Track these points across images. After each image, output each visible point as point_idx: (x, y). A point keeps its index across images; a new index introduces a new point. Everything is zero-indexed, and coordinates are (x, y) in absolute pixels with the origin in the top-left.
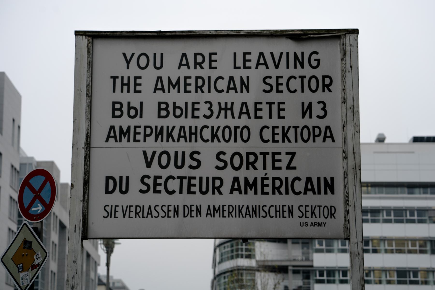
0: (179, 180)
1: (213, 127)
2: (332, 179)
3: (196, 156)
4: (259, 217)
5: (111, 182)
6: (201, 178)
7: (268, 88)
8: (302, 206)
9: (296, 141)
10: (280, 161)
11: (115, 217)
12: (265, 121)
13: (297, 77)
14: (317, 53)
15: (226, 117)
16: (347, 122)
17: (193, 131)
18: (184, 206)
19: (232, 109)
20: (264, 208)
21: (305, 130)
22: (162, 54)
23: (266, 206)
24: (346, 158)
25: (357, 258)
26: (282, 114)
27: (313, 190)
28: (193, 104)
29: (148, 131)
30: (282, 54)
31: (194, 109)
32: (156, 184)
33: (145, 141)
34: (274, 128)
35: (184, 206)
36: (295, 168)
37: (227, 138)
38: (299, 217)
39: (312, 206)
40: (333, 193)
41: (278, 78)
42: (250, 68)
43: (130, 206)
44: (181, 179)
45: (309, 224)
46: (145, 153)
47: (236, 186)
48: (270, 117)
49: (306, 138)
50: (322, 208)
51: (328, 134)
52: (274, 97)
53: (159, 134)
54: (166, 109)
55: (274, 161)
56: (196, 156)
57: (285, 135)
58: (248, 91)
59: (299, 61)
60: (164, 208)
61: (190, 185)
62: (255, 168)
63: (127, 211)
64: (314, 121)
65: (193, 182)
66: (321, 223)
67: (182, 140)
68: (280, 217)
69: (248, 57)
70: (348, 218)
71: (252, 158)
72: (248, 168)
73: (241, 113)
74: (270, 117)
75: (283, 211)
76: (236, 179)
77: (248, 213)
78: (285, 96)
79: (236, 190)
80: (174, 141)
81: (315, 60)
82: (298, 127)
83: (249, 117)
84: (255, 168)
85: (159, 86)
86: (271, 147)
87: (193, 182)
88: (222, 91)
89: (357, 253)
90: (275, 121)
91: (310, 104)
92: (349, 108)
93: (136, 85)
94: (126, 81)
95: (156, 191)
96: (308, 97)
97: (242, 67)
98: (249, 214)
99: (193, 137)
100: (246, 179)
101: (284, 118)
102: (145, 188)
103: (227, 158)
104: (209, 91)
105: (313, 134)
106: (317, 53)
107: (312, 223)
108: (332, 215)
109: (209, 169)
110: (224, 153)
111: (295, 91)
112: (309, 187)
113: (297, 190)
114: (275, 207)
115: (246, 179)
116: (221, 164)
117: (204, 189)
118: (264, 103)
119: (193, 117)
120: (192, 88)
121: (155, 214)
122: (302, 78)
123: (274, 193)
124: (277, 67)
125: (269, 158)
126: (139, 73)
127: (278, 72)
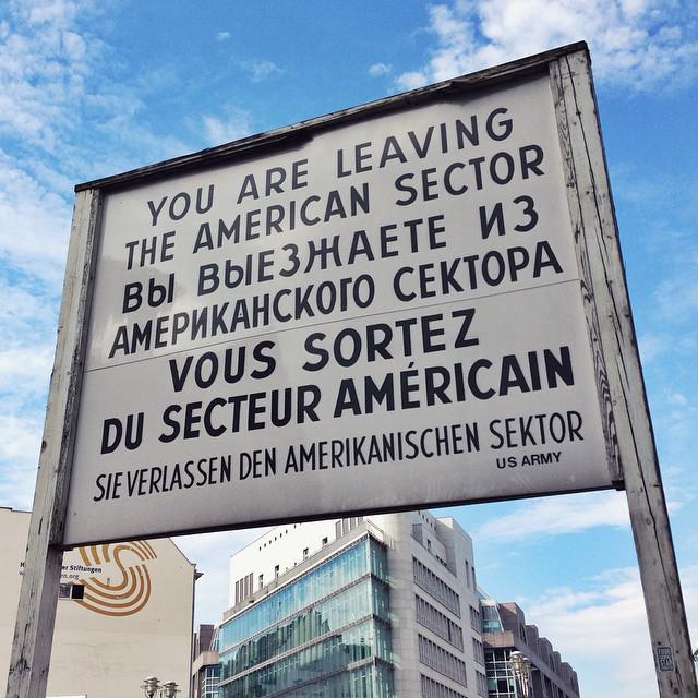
0: (233, 404)
1: (298, 291)
2: (565, 351)
3: (265, 352)
4: (401, 458)
5: (113, 429)
6: (275, 394)
7: (407, 196)
8: (499, 421)
9: (474, 286)
10: (441, 332)
11: (115, 497)
12: (406, 258)
13: (466, 163)
14: (503, 111)
15: (324, 266)
16: (582, 223)
17: (261, 305)
18: (242, 455)
19: (335, 250)
20: (411, 437)
21: (493, 262)
22: (212, 188)
23: (414, 432)
24: (589, 298)
25: (650, 528)
26: (439, 238)
27: (521, 382)
28: (262, 255)
29: (181, 321)
30: (431, 130)
31: (262, 265)
32: (190, 420)
33: (174, 342)
34: (423, 269)
35: (242, 455)
36: (475, 342)
37: (326, 305)
38: (493, 446)
39: (521, 419)
40: (569, 381)
41: (425, 173)
42: (370, 168)
43: (142, 471)
44: (237, 401)
45: (519, 461)
46: (173, 363)
47: (347, 399)
48: (415, 249)
49: (494, 275)
50: (546, 421)
51: (546, 258)
52: (421, 210)
53: (198, 324)
54: (214, 277)
55: (427, 334)
56: (265, 352)
57: (448, 279)
58: (367, 211)
59: (468, 134)
60: (203, 466)
61: (253, 411)
62: (387, 356)
63: (136, 483)
64: (513, 239)
65: (259, 403)
66: (549, 455)
67: (241, 325)
68: (447, 453)
69: (364, 152)
70: (613, 432)
71: (379, 336)
72: (371, 358)
73: (354, 252)
74: (415, 249)
75: (455, 439)
76: (347, 385)
77: (374, 453)
78: (444, 203)
79: (348, 406)
80: (225, 331)
81: (501, 124)
82: (477, 257)
83: (371, 257)
84: (387, 356)
85: (204, 239)
86: (418, 308)
87: (259, 403)
88: (317, 220)
89: (647, 515)
90: (426, 255)
91: (499, 207)
92: (585, 194)
93: (165, 246)
94: (149, 246)
95: (190, 434)
96: (491, 194)
97: (354, 171)
98: (378, 455)
99: (261, 315)
100: (368, 380)
101: (443, 245)
102: (170, 431)
103: (327, 345)
104: (292, 227)
105: (511, 265)
106: (503, 111)
107: (525, 457)
108: (574, 432)
109: (291, 371)
110: (321, 336)
111: (464, 189)
112: (512, 377)
113: (483, 389)
114: (434, 432)
115: (368, 380)
116: (316, 359)
117: (281, 416)
118: (400, 226)
119: (262, 278)
120: (260, 230)
121: (186, 479)
122: (476, 162)
123: (431, 402)
124: (422, 154)
125: (416, 332)
126: (171, 225)
127: (426, 163)
